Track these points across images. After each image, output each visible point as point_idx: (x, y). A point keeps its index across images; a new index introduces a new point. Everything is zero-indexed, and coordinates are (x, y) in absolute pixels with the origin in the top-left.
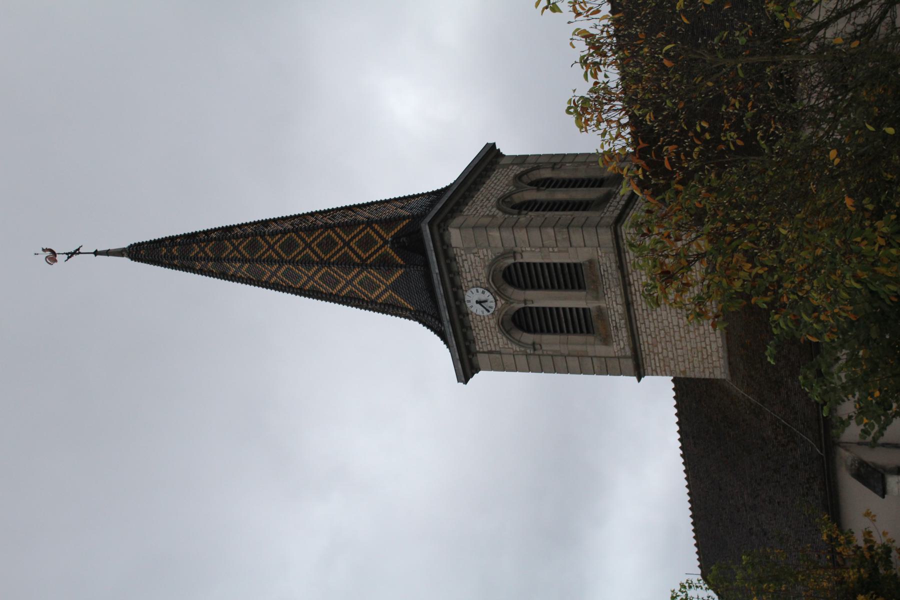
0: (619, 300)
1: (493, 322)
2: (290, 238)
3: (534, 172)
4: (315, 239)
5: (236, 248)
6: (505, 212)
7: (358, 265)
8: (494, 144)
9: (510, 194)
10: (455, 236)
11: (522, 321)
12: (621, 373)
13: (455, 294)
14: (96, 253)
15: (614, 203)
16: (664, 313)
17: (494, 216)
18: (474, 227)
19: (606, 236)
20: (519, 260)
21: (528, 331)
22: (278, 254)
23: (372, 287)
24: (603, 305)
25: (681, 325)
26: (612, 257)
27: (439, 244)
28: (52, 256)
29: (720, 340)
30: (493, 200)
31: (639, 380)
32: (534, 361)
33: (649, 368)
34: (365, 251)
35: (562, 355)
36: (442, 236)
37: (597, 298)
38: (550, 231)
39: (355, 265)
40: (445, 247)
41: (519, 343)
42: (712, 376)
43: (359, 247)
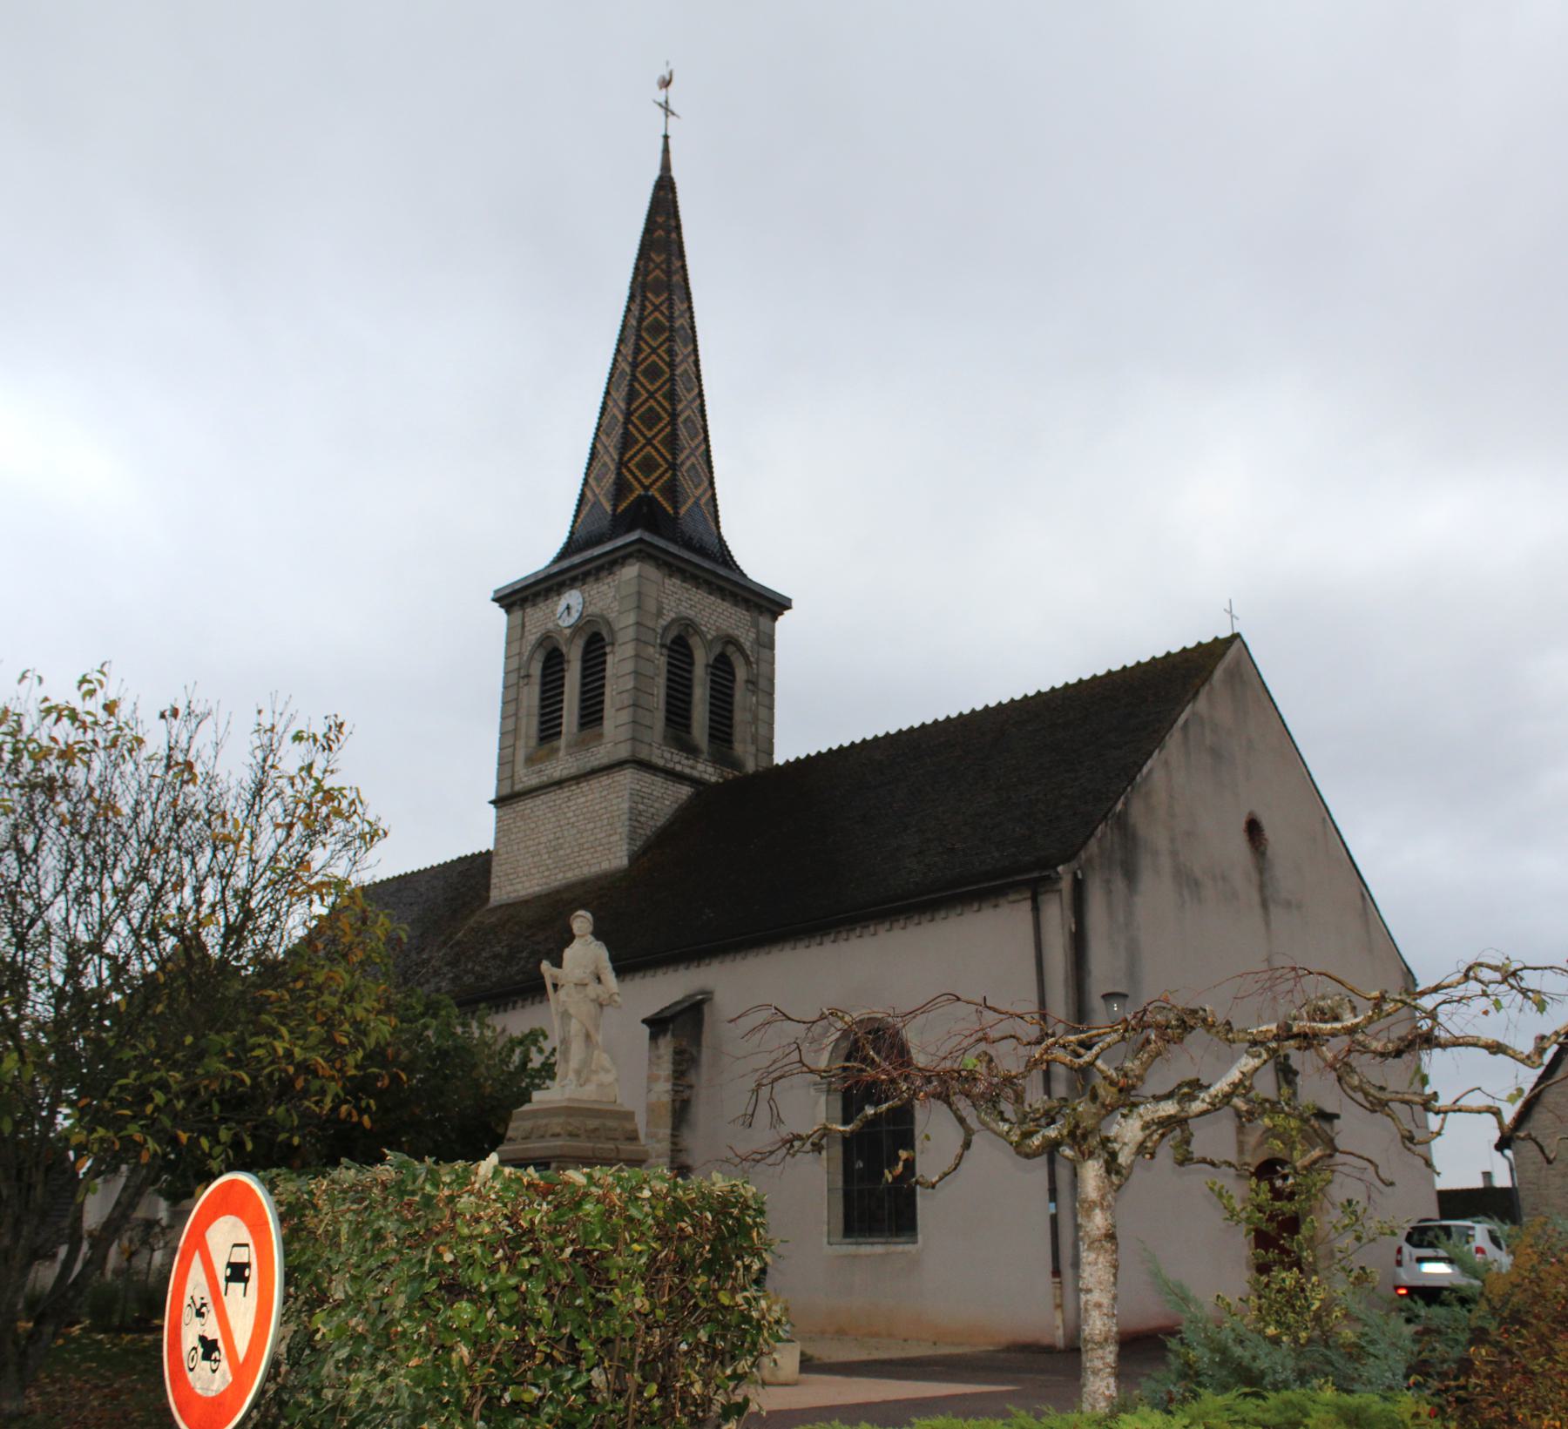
1: (550, 626)
2: (663, 372)
4: (659, 403)
5: (656, 308)
6: (666, 629)
7: (621, 459)
9: (701, 635)
10: (630, 571)
11: (553, 660)
12: (500, 780)
13: (574, 580)
14: (666, 137)
15: (676, 758)
17: (659, 614)
18: (639, 593)
19: (624, 752)
20: (608, 649)
21: (544, 668)
22: (645, 359)
23: (598, 479)
24: (562, 753)
26: (606, 761)
27: (622, 553)
28: (666, 83)
29: (523, 893)
30: (691, 613)
32: (514, 678)
34: (638, 466)
35: (517, 709)
36: (630, 555)
37: (568, 746)
38: (631, 685)
39: (622, 455)
41: (531, 658)
43: (644, 457)
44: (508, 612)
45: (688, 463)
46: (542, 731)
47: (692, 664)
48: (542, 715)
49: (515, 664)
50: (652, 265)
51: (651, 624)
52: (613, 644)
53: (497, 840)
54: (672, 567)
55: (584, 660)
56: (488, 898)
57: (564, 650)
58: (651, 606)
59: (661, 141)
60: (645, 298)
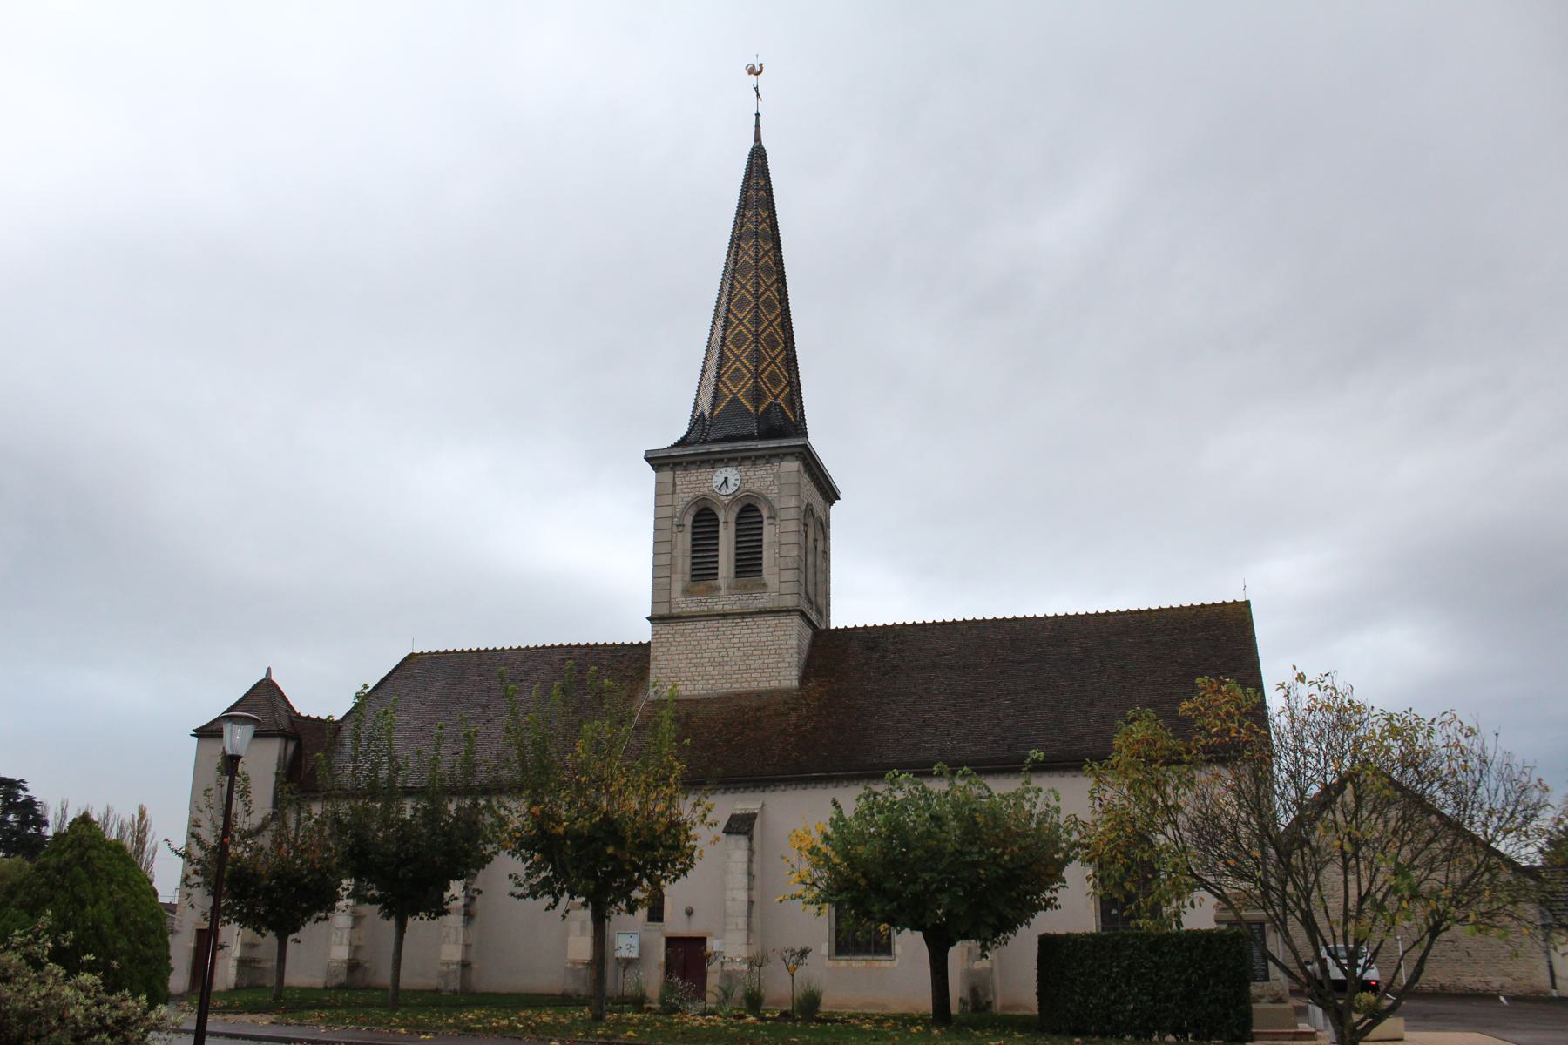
0: (727, 607)
1: (705, 490)
11: (704, 517)
13: (735, 459)
14: (758, 115)
19: (790, 602)
26: (770, 605)
32: (667, 524)
36: (792, 454)
41: (684, 512)
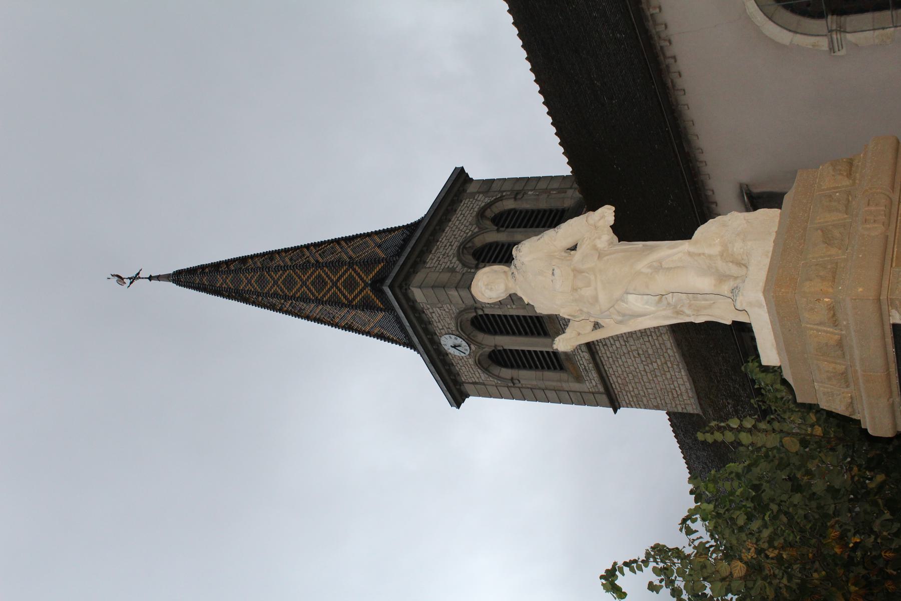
1: (471, 361)
3: (499, 204)
5: (249, 282)
6: (464, 265)
8: (462, 168)
9: (474, 236)
10: (418, 295)
14: (151, 278)
16: (629, 361)
17: (452, 270)
18: (433, 287)
20: (480, 312)
21: (506, 366)
25: (648, 370)
27: (404, 302)
28: (120, 278)
29: (688, 384)
31: (615, 412)
32: (515, 391)
33: (624, 403)
35: (540, 389)
39: (343, 305)
40: (411, 304)
41: (498, 377)
42: (685, 411)
44: (468, 396)
45: (351, 253)
46: (555, 368)
47: (497, 244)
48: (543, 368)
49: (504, 390)
50: (224, 285)
51: (459, 276)
52: (476, 308)
53: (657, 408)
54: (417, 262)
55: (495, 333)
56: (698, 415)
57: (488, 350)
58: (445, 277)
59: (154, 282)
60: (267, 295)
